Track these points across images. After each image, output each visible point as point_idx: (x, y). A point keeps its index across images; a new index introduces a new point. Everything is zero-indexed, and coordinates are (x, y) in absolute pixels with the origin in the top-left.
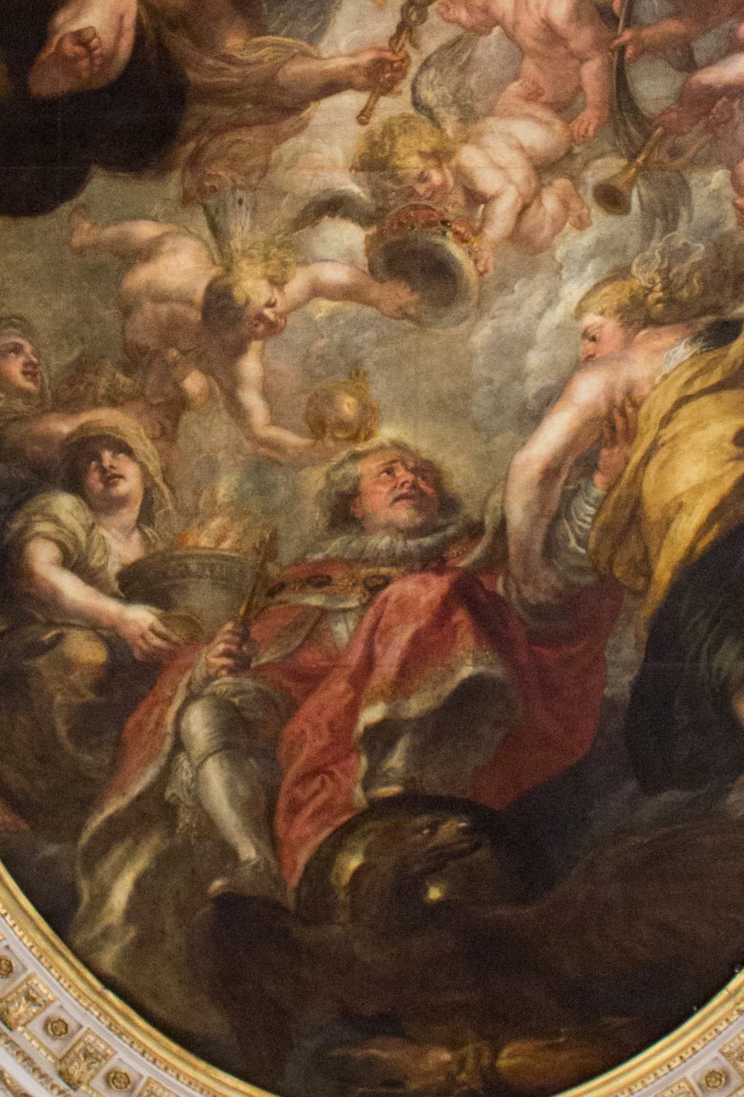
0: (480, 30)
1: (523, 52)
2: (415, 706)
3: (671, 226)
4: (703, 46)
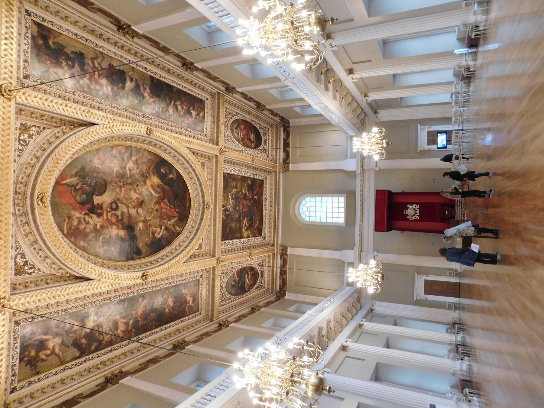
0: (125, 198)
1: (126, 194)
3: (139, 180)
4: (127, 176)
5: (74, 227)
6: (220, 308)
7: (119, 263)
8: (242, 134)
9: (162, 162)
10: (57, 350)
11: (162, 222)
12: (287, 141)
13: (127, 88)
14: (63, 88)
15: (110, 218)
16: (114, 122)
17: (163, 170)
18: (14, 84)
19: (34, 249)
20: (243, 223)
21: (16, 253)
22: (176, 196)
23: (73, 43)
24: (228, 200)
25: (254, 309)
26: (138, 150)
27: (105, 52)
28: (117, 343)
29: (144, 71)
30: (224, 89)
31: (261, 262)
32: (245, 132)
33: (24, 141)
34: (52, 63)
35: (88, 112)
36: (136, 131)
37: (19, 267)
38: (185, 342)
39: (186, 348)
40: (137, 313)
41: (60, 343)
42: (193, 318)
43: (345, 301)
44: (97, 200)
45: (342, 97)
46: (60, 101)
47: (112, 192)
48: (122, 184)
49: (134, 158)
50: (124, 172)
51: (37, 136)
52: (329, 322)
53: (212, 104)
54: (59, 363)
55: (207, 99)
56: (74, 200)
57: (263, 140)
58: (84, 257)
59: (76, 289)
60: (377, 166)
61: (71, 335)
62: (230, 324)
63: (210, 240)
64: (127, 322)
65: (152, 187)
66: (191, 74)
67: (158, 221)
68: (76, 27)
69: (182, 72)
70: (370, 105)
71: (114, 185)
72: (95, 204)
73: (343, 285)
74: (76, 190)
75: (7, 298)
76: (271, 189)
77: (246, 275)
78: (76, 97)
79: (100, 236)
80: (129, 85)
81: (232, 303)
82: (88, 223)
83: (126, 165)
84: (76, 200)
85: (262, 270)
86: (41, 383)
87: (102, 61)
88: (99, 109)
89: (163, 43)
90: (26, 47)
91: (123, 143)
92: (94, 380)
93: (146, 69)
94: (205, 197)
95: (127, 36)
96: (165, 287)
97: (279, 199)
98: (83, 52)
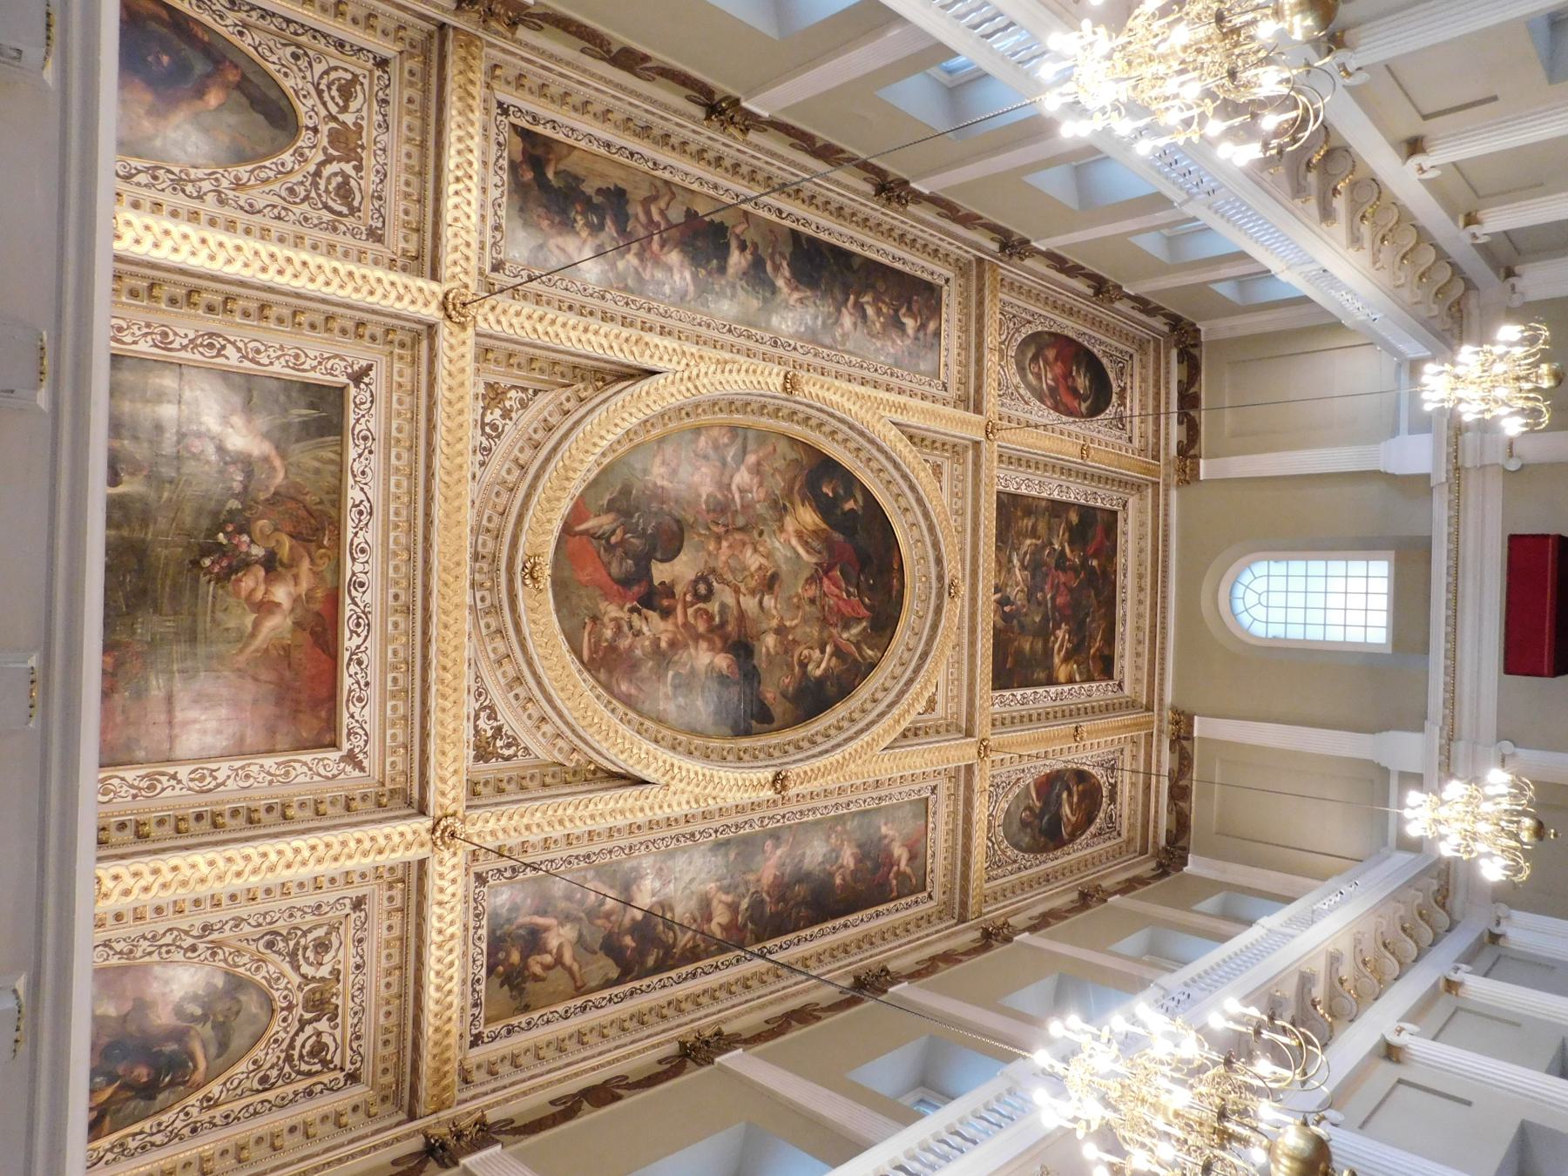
0: (729, 567)
2: (843, 585)
3: (765, 519)
4: (733, 508)
5: (605, 644)
6: (986, 886)
7: (715, 743)
8: (1049, 375)
9: (825, 467)
10: (568, 957)
11: (825, 635)
12: (1192, 390)
13: (731, 271)
14: (578, 284)
15: (692, 620)
16: (702, 364)
17: (827, 490)
18: (473, 287)
19: (517, 697)
20: (1057, 638)
21: (477, 706)
22: (864, 561)
23: (600, 167)
24: (1009, 571)
25: (1087, 898)
26: (763, 436)
27: (677, 179)
28: (709, 955)
29: (774, 218)
30: (995, 247)
31: (1111, 757)
32: (1059, 368)
33: (494, 427)
34: (552, 225)
35: (637, 342)
36: (755, 383)
37: (483, 740)
38: (888, 973)
39: (891, 990)
40: (758, 880)
41: (575, 940)
42: (908, 906)
43: (1393, 897)
44: (661, 572)
45: (1380, 236)
46: (573, 319)
47: (698, 551)
48: (721, 530)
49: (751, 459)
50: (726, 496)
51: (521, 412)
52: (1334, 959)
53: (962, 293)
54: (571, 989)
55: (947, 281)
56: (604, 573)
57: (1115, 389)
58: (629, 722)
59: (612, 804)
60: (1511, 456)
61: (599, 922)
62: (1016, 935)
63: (960, 685)
64: (733, 902)
65: (800, 535)
66: (901, 214)
67: (814, 631)
68: (607, 124)
69: (876, 210)
70: (1486, 251)
71: (703, 532)
72: (656, 582)
73: (1385, 844)
74: (610, 548)
75: (460, 815)
76: (1142, 537)
77: (1065, 795)
78: (609, 306)
79: (667, 669)
80: (737, 260)
81: (1022, 874)
82: (638, 633)
83: (732, 477)
84: (609, 575)
85: (1112, 781)
86: (535, 1033)
87: (668, 205)
88: (663, 332)
89: (823, 136)
90: (497, 193)
91: (723, 417)
92: (653, 1047)
93: (780, 211)
94: (945, 564)
95: (731, 129)
96: (832, 813)
97: (1165, 572)
98: (622, 185)
